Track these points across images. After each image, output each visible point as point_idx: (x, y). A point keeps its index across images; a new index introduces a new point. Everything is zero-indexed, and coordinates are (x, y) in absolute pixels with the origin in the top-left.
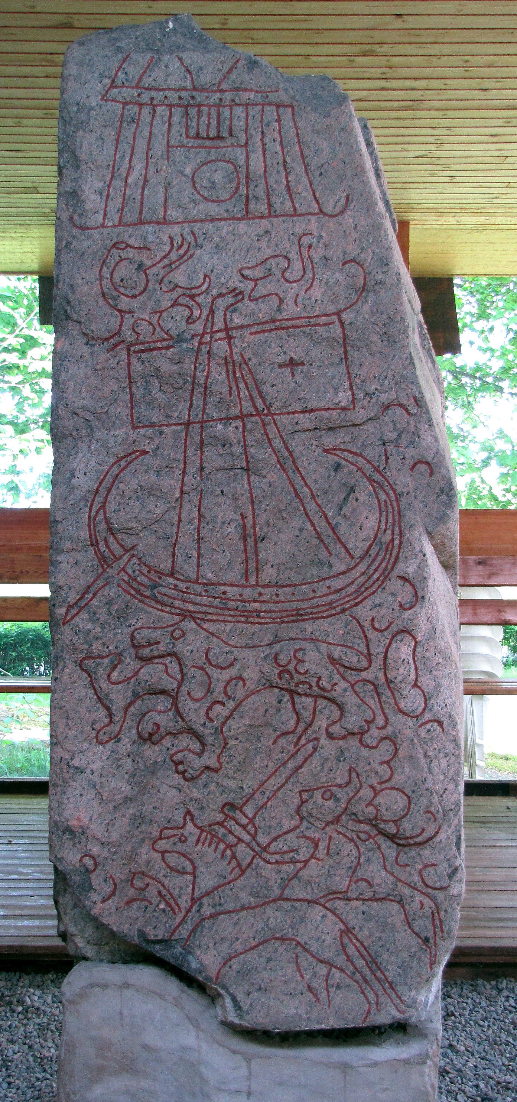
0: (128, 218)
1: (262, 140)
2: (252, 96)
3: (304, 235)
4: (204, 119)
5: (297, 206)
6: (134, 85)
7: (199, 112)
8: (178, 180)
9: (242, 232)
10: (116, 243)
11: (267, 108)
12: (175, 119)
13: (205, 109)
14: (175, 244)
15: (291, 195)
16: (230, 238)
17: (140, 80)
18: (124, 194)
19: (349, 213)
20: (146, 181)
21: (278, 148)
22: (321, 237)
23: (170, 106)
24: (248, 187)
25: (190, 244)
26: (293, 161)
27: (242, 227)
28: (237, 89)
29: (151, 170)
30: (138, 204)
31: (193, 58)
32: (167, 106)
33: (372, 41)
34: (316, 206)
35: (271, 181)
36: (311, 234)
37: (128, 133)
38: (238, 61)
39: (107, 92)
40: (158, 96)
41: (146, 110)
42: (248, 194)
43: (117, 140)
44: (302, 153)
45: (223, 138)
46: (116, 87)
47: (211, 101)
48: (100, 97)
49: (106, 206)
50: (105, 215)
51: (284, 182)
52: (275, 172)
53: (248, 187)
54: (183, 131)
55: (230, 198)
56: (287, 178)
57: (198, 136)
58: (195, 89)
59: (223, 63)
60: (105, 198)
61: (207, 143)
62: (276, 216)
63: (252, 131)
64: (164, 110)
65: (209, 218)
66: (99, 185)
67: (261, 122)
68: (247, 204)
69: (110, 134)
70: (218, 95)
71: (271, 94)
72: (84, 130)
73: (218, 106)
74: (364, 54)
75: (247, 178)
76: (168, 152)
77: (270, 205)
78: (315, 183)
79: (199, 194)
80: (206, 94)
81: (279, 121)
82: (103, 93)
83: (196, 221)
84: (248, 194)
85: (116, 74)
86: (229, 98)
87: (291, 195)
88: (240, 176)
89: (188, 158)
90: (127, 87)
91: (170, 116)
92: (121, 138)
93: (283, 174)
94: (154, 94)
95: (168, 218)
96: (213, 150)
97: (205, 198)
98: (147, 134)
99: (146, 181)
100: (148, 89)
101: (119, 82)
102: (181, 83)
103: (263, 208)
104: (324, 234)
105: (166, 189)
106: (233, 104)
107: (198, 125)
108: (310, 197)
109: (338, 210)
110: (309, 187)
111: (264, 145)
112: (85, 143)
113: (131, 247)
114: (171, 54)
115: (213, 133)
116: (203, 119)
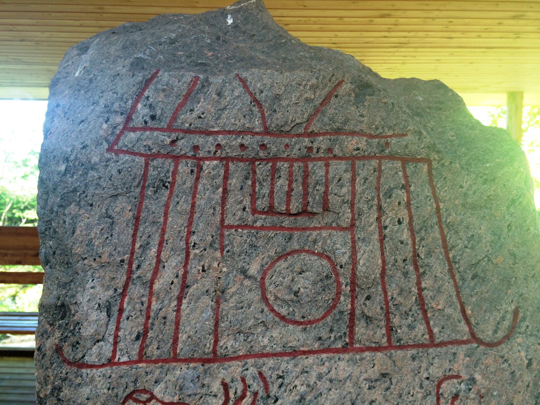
0: (153, 351)
1: (378, 219)
2: (362, 143)
3: (447, 378)
4: (282, 183)
5: (436, 330)
6: (164, 125)
7: (274, 171)
8: (237, 286)
9: (342, 375)
10: (133, 392)
11: (387, 165)
12: (234, 182)
13: (284, 166)
14: (232, 395)
15: (425, 312)
16: (323, 385)
17: (174, 118)
18: (149, 306)
19: (519, 340)
20: (185, 286)
21: (406, 235)
22: (473, 380)
23: (226, 160)
24: (353, 298)
25: (256, 394)
26: (429, 254)
27: (343, 366)
28: (338, 131)
29: (194, 268)
30: (169, 329)
31: (263, 79)
32: (221, 159)
33: (393, 8)
34: (467, 329)
35: (393, 291)
36: (458, 377)
37: (154, 206)
38: (340, 84)
39: (119, 137)
40: (207, 144)
41: (184, 168)
42: (353, 309)
43: (137, 219)
44: (444, 241)
45: (314, 214)
46: (134, 130)
47: (295, 152)
48: (106, 146)
49: (118, 329)
50: (115, 343)
51: (415, 290)
52: (399, 274)
53: (353, 298)
54: (247, 202)
55: (323, 318)
56: (419, 283)
57: (271, 210)
58: (267, 132)
59: (314, 88)
60: (116, 314)
61: (287, 222)
62: (401, 347)
63: (361, 205)
64: (217, 166)
65: (289, 350)
66: (105, 295)
67: (378, 189)
68: (351, 327)
69: (123, 208)
70: (306, 141)
71: (394, 141)
72: (78, 204)
73: (305, 159)
74: (382, 16)
75: (353, 283)
76: (222, 235)
77: (390, 329)
78: (465, 292)
79: (272, 310)
80: (287, 140)
81: (406, 187)
82: (112, 139)
83: (267, 355)
84: (353, 309)
85: (134, 107)
86: (324, 147)
87: (425, 312)
88: (342, 280)
89: (253, 246)
90: (151, 129)
91: (226, 178)
92: (143, 215)
93: (413, 277)
94: (199, 140)
95: (220, 351)
96: (296, 234)
97: (283, 318)
98: (186, 207)
99: (185, 286)
100: (188, 131)
101: (137, 121)
102: (242, 123)
103: (380, 335)
104: (478, 377)
105: (218, 303)
106: (330, 156)
107: (272, 192)
108: (457, 315)
109: (500, 334)
110: (455, 299)
111: (382, 228)
112: (81, 225)
113: (158, 400)
114: (229, 71)
115: (295, 207)
116: (279, 183)
